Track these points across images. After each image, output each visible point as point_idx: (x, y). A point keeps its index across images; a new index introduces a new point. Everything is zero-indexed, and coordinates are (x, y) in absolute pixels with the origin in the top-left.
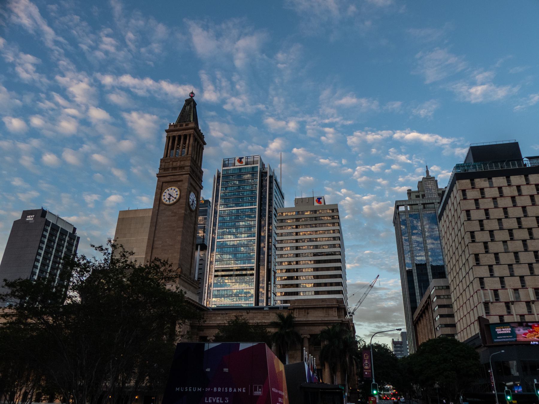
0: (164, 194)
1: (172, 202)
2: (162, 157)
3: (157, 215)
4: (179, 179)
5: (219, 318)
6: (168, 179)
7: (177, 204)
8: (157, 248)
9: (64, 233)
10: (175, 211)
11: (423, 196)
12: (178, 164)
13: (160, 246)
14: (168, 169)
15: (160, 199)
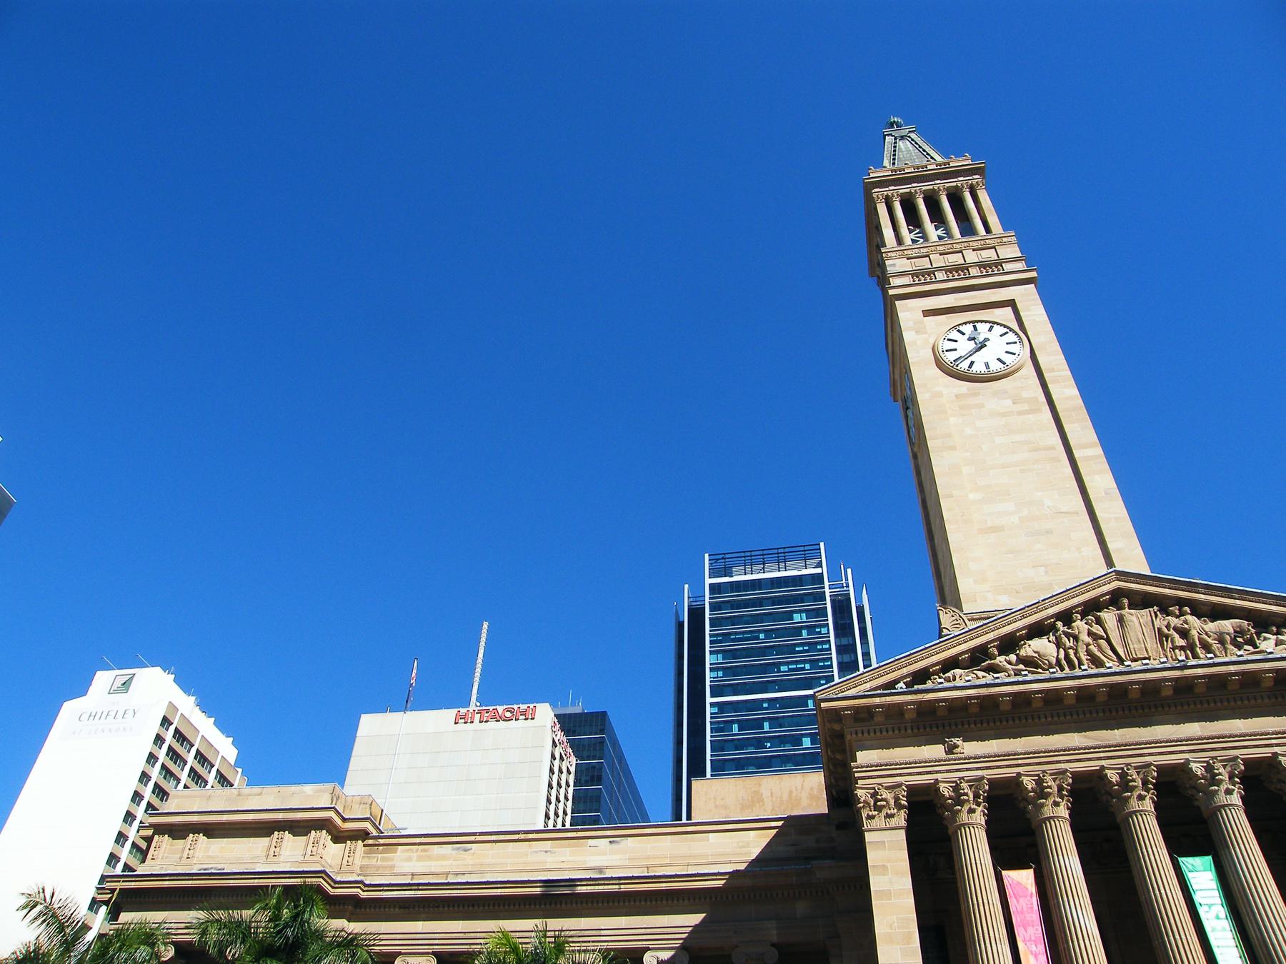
10: (1025, 394)
12: (971, 257)
14: (931, 272)
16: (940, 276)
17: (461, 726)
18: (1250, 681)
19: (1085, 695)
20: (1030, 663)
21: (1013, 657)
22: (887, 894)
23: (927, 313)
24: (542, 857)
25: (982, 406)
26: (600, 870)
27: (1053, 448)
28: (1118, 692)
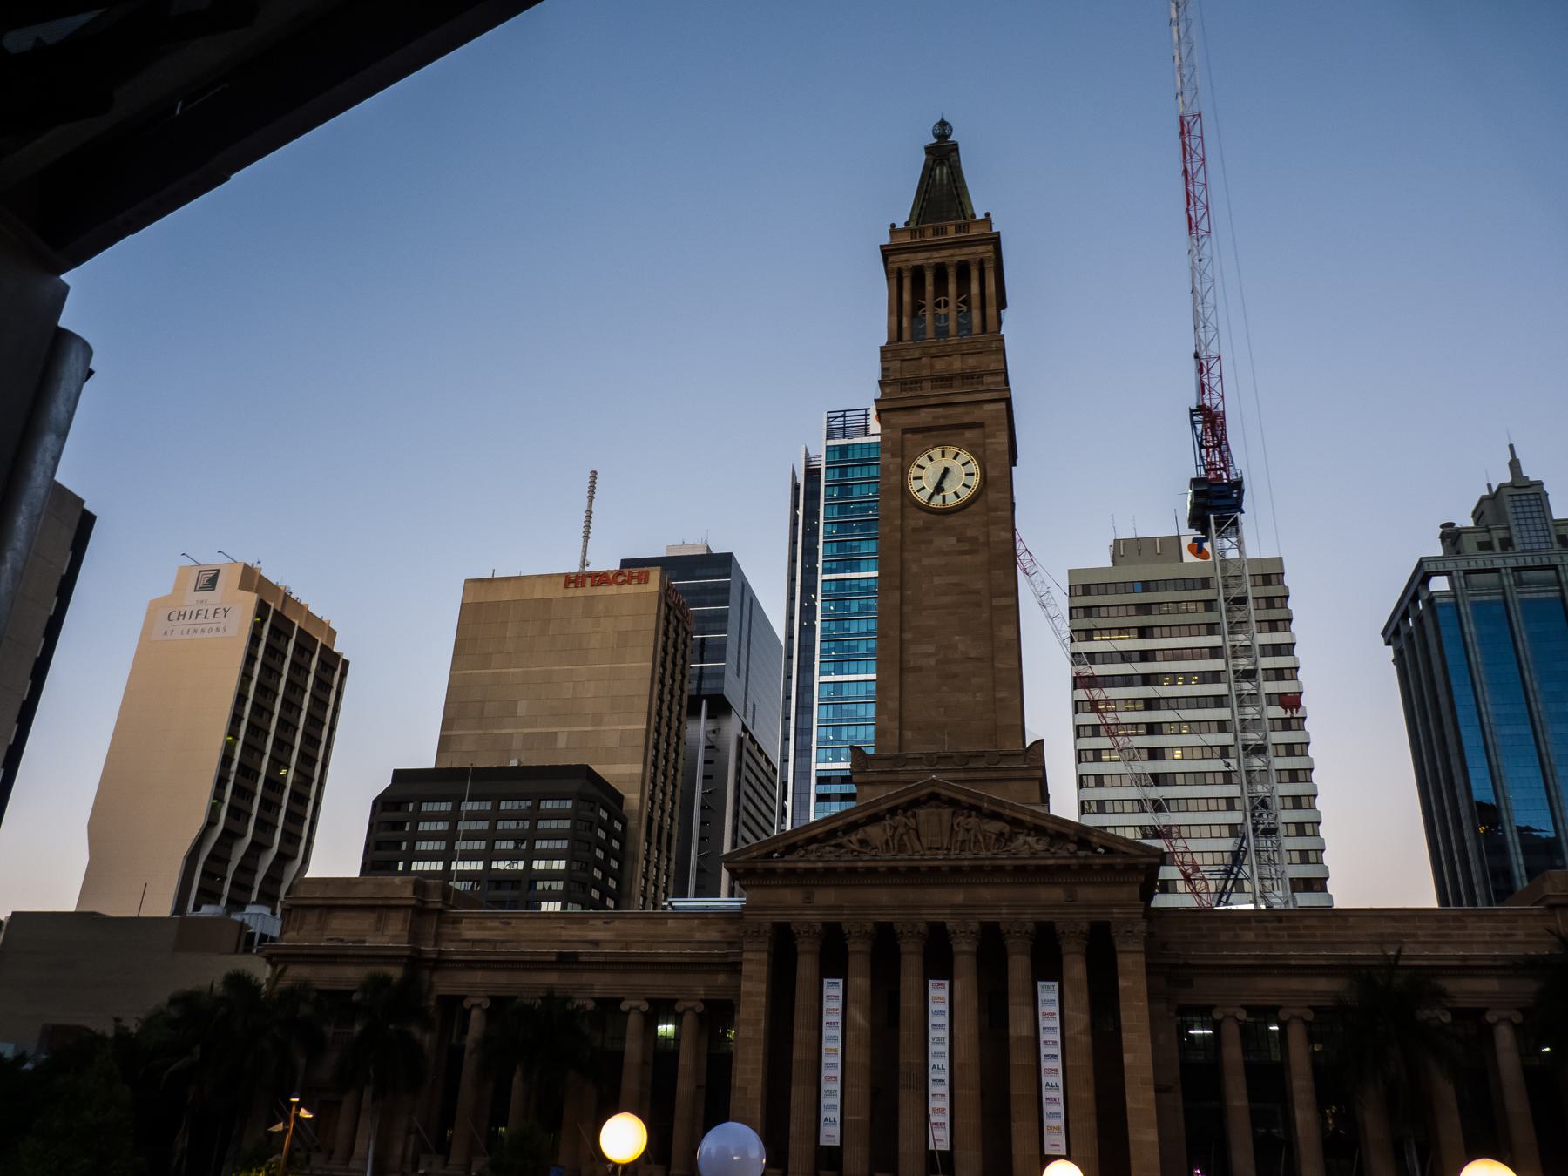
0: (914, 472)
1: (952, 501)
2: (884, 341)
3: (902, 551)
4: (967, 420)
5: (1249, 936)
6: (924, 417)
7: (973, 508)
8: (918, 669)
9: (306, 644)
10: (970, 533)
11: (1507, 544)
12: (957, 364)
13: (932, 661)
14: (917, 382)
15: (904, 489)
16: (927, 388)
17: (574, 592)
18: (1000, 869)
19: (893, 871)
20: (862, 842)
21: (853, 838)
22: (749, 994)
23: (904, 431)
24: (557, 931)
25: (930, 542)
26: (596, 943)
27: (978, 592)
28: (914, 870)
